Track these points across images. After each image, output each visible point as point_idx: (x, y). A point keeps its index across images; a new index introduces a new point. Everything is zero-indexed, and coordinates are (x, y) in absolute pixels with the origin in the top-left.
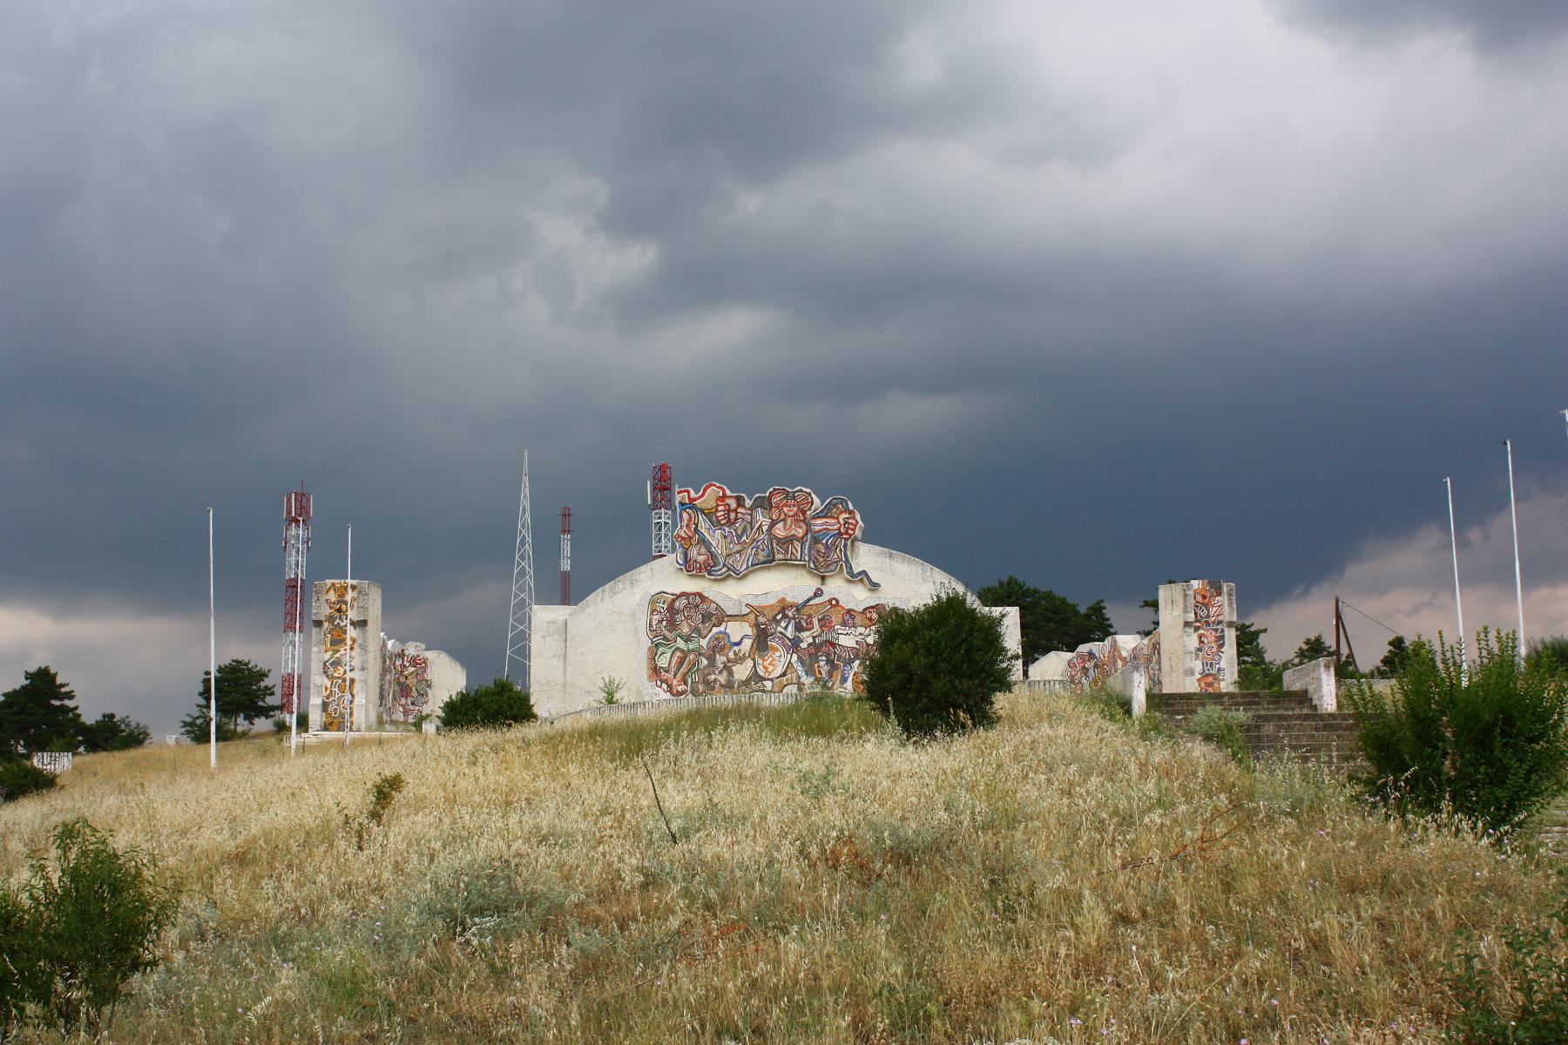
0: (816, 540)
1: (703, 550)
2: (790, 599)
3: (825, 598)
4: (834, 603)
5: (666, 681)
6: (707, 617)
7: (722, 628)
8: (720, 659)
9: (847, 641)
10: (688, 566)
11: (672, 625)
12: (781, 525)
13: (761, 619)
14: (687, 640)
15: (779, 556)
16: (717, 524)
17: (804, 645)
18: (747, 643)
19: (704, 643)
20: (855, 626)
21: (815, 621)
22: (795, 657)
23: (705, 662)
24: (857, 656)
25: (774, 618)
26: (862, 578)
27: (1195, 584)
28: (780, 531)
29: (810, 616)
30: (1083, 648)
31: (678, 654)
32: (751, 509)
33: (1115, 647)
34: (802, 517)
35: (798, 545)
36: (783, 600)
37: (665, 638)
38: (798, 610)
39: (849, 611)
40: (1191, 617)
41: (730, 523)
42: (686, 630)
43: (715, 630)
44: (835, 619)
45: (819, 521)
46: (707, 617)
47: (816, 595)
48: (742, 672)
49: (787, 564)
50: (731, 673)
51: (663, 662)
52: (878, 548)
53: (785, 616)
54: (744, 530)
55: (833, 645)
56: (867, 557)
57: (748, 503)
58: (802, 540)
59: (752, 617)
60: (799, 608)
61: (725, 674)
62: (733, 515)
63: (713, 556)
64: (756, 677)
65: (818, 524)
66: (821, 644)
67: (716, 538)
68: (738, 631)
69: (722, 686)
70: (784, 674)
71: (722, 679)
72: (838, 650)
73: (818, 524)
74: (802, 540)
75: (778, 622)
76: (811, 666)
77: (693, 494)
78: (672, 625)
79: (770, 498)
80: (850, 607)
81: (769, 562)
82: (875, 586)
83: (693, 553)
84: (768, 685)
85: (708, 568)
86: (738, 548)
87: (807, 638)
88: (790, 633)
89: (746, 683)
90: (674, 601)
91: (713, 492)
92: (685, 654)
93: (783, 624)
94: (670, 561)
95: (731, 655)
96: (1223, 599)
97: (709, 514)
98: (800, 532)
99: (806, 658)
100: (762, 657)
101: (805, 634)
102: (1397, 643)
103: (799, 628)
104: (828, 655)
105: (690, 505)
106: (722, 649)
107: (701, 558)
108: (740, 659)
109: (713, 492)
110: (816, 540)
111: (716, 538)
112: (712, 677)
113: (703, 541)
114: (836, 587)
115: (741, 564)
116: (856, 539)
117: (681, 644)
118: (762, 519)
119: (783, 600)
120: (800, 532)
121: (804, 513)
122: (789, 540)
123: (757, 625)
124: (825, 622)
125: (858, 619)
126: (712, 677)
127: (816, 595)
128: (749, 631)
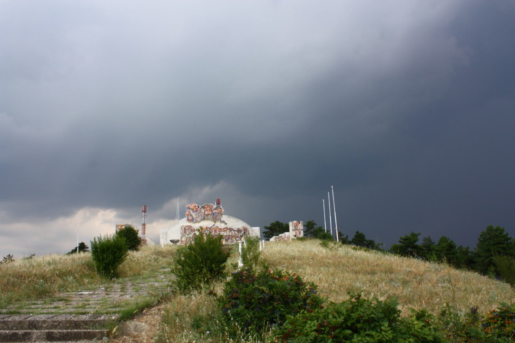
0: (214, 214)
4: (217, 227)
6: (192, 230)
10: (188, 220)
11: (185, 232)
14: (188, 235)
16: (194, 212)
19: (191, 236)
26: (223, 222)
27: (295, 222)
28: (206, 213)
30: (280, 235)
33: (285, 235)
34: (211, 210)
40: (294, 228)
41: (196, 211)
46: (192, 230)
49: (207, 219)
56: (224, 218)
57: (200, 207)
60: (210, 228)
63: (193, 218)
65: (214, 211)
67: (194, 215)
73: (214, 211)
74: (211, 215)
78: (185, 232)
81: (204, 219)
82: (226, 224)
83: (189, 217)
85: (192, 220)
91: (193, 205)
92: (187, 238)
94: (185, 219)
96: (300, 225)
97: (192, 210)
98: (210, 213)
102: (357, 232)
105: (189, 208)
109: (193, 205)
110: (214, 214)
111: (194, 215)
113: (191, 215)
114: (218, 224)
115: (199, 219)
116: (222, 214)
117: (187, 236)
118: (203, 210)
122: (208, 215)
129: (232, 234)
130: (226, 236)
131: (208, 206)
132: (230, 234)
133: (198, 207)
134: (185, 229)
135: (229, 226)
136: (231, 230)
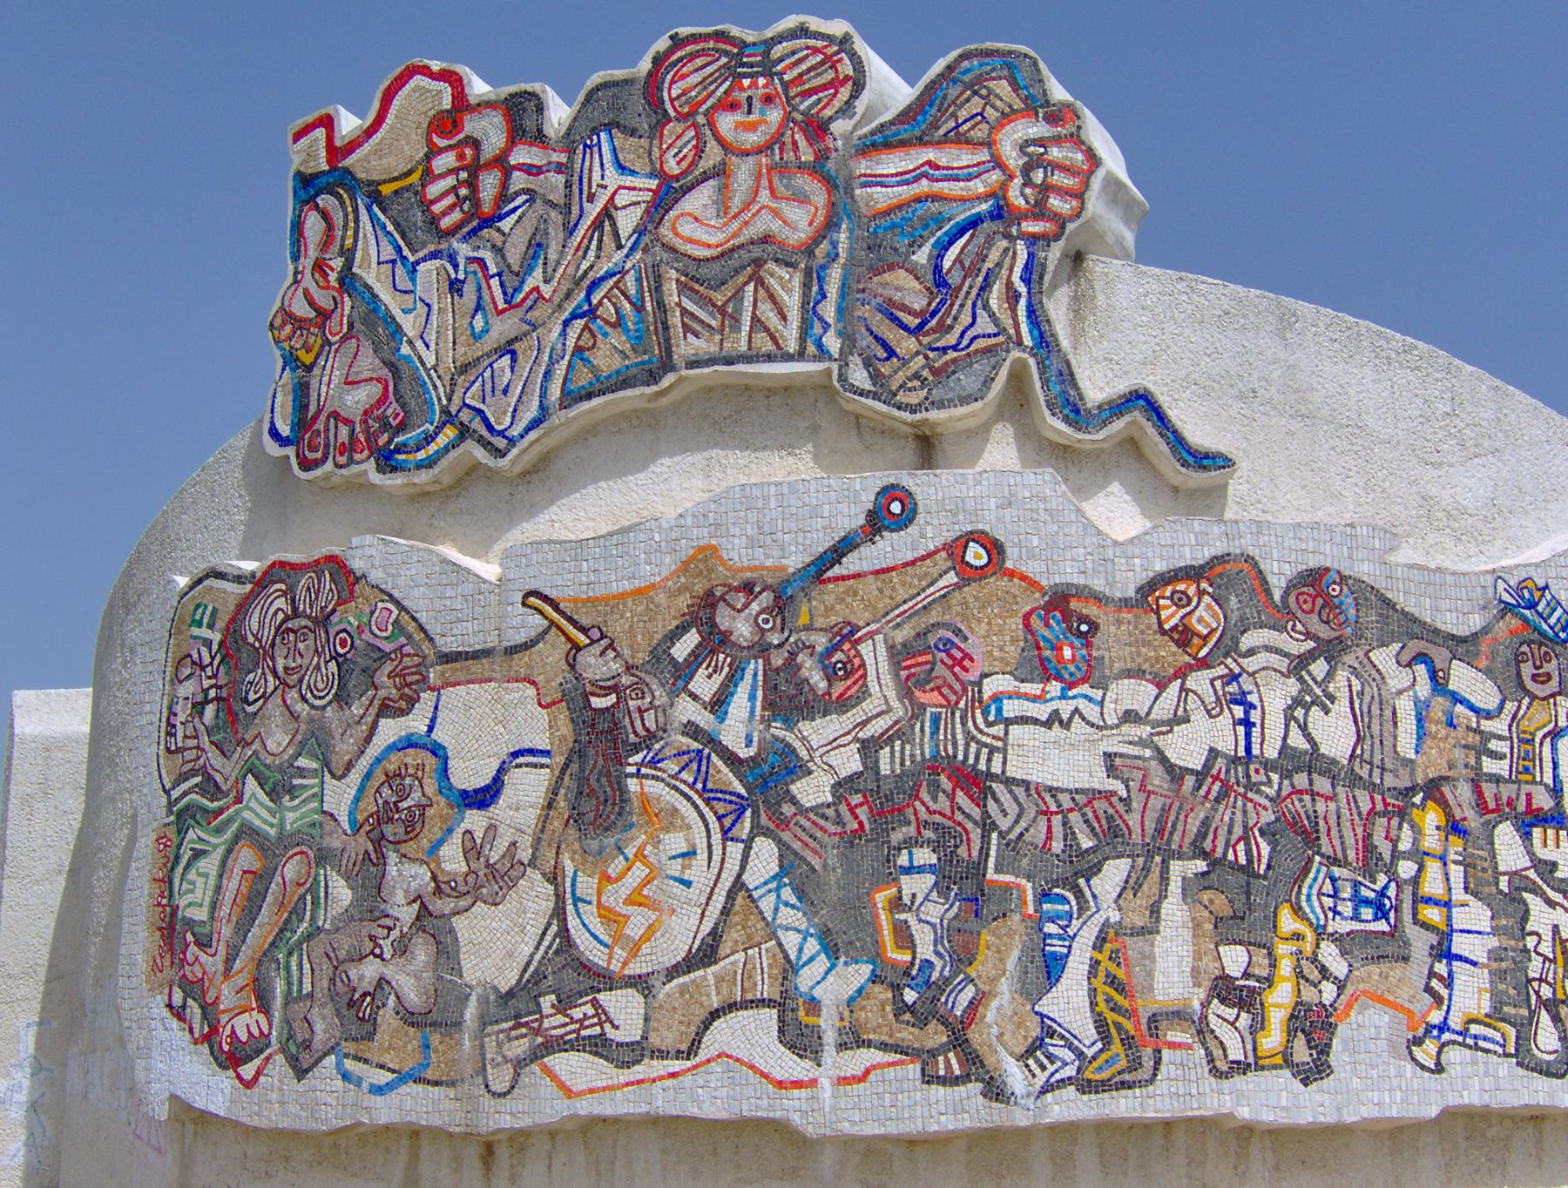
0: (878, 255)
1: (368, 363)
2: (739, 553)
3: (929, 533)
4: (978, 557)
5: (195, 988)
7: (416, 723)
8: (405, 877)
9: (1054, 754)
12: (700, 200)
13: (596, 665)
15: (687, 347)
17: (812, 790)
18: (528, 789)
19: (340, 797)
20: (1091, 674)
21: (874, 656)
22: (765, 855)
23: (342, 893)
24: (1112, 836)
25: (660, 654)
26: (1146, 440)
28: (698, 224)
29: (847, 635)
31: (246, 857)
32: (569, 141)
35: (788, 286)
36: (707, 555)
37: (211, 787)
38: (782, 606)
39: (1060, 601)
42: (277, 739)
43: (390, 730)
44: (993, 638)
45: (892, 163)
47: (877, 522)
48: (497, 943)
50: (446, 952)
51: (194, 901)
52: (1216, 293)
53: (715, 641)
54: (536, 247)
55: (975, 782)
57: (558, 114)
58: (808, 260)
59: (553, 652)
61: (422, 952)
62: (489, 184)
64: (567, 974)
66: (910, 783)
68: (488, 727)
69: (410, 1018)
70: (707, 953)
71: (410, 980)
72: (1004, 808)
75: (683, 673)
76: (857, 908)
77: (348, 124)
78: (233, 714)
79: (653, 82)
80: (1068, 574)
84: (625, 1012)
86: (504, 328)
87: (829, 749)
88: (739, 728)
89: (515, 1004)
90: (243, 606)
92: (272, 849)
93: (705, 684)
95: (453, 859)
98: (797, 222)
99: (826, 859)
100: (595, 859)
101: (817, 731)
103: (788, 701)
104: (946, 838)
106: (412, 826)
107: (357, 400)
108: (491, 878)
112: (369, 971)
113: (377, 326)
115: (512, 398)
117: (256, 808)
119: (707, 555)
120: (798, 222)
121: (817, 129)
123: (575, 697)
124: (932, 661)
125: (1114, 639)
126: (369, 971)
127: (877, 522)
128: (537, 726)
129: (1370, 718)
130: (1223, 777)
131: (740, 60)
132: (1334, 734)
133: (520, 114)
134: (234, 648)
135: (1283, 511)
136: (1331, 611)
